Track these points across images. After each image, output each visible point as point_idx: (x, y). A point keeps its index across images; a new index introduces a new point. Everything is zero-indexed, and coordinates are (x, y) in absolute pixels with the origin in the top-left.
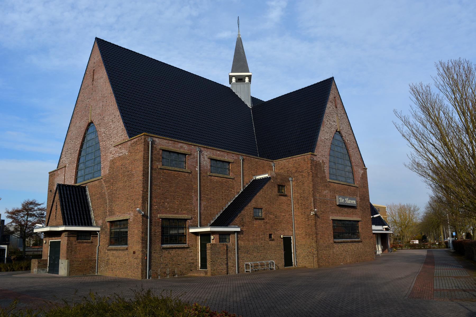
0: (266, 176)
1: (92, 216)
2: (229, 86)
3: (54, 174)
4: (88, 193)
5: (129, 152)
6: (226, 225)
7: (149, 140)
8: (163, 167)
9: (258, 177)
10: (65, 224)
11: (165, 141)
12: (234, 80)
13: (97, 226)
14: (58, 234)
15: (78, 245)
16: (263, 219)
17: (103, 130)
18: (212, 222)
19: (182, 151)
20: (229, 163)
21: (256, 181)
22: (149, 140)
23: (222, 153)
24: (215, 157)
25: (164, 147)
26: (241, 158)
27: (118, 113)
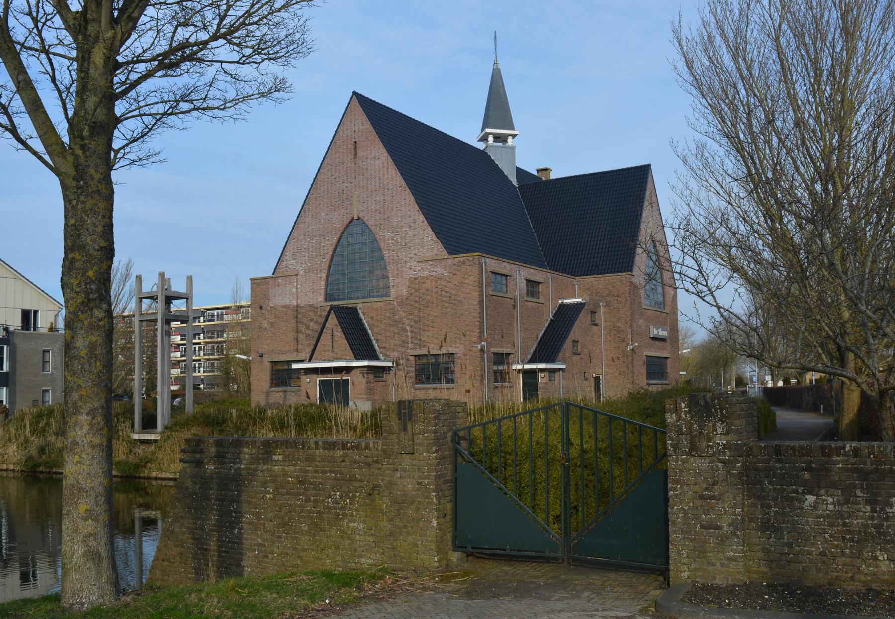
0: (579, 300)
1: (377, 348)
2: (481, 146)
3: (268, 283)
4: (361, 315)
5: (450, 272)
6: (552, 361)
7: (483, 261)
8: (493, 293)
9: (566, 301)
10: (357, 357)
11: (493, 261)
12: (491, 139)
13: (386, 360)
14: (348, 369)
15: (376, 383)
16: (579, 354)
17: (388, 235)
18: (529, 357)
19: (504, 272)
20: (540, 283)
21: (562, 306)
22: (483, 261)
23: (535, 272)
24: (532, 278)
25: (493, 269)
26: (550, 276)
27: (421, 217)
